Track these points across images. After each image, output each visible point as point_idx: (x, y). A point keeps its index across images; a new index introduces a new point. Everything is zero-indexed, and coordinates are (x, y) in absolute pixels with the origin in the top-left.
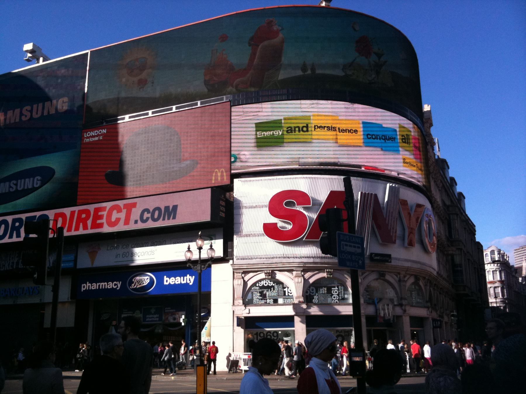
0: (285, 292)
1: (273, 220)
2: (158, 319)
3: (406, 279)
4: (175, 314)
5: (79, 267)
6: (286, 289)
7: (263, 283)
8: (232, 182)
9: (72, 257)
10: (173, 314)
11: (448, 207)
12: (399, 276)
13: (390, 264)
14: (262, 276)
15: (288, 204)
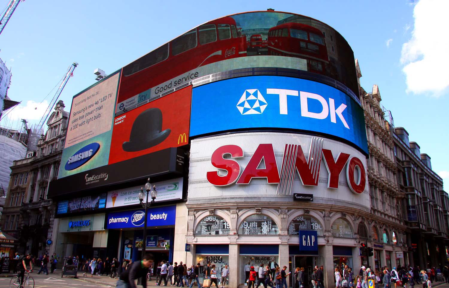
0: (224, 225)
1: (214, 169)
2: (154, 245)
3: (331, 215)
4: (164, 242)
5: (106, 208)
6: (225, 224)
7: (209, 219)
8: (190, 143)
9: (104, 201)
10: (163, 241)
11: (403, 162)
12: (324, 212)
13: (312, 202)
14: (208, 213)
15: (225, 157)
